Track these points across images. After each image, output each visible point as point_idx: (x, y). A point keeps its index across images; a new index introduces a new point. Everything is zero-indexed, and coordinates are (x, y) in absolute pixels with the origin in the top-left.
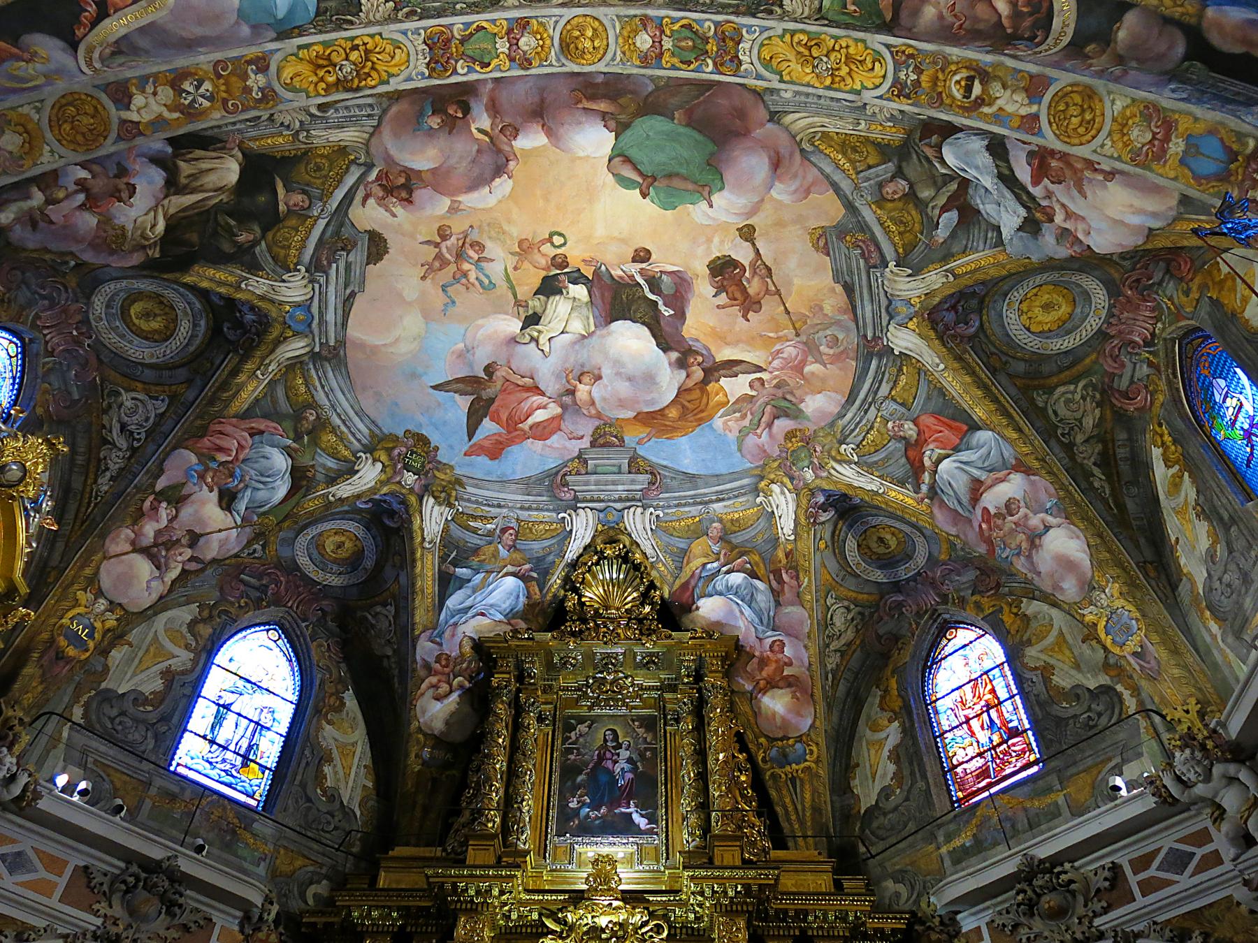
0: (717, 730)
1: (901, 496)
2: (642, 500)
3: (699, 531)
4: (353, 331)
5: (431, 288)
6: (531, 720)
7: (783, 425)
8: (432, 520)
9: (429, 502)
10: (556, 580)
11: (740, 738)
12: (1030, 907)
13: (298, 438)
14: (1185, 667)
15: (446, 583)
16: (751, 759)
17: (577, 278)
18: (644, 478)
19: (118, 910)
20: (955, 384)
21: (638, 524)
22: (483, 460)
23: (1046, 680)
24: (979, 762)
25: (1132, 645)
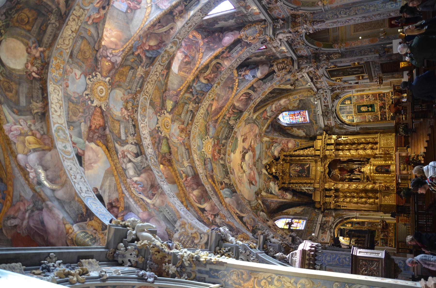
0: (297, 153)
1: (269, 121)
2: (262, 161)
3: (266, 153)
4: (247, 198)
5: (242, 185)
6: (292, 181)
7: (257, 137)
8: (264, 193)
9: (262, 194)
10: (270, 177)
11: (294, 151)
12: (327, 116)
13: (258, 210)
14: (303, 92)
15: (271, 193)
16: (298, 150)
17: (241, 163)
18: (259, 160)
19: (326, 229)
20: (261, 111)
21: (264, 162)
22: (257, 184)
23: (295, 107)
24: (303, 118)
25: (298, 97)
